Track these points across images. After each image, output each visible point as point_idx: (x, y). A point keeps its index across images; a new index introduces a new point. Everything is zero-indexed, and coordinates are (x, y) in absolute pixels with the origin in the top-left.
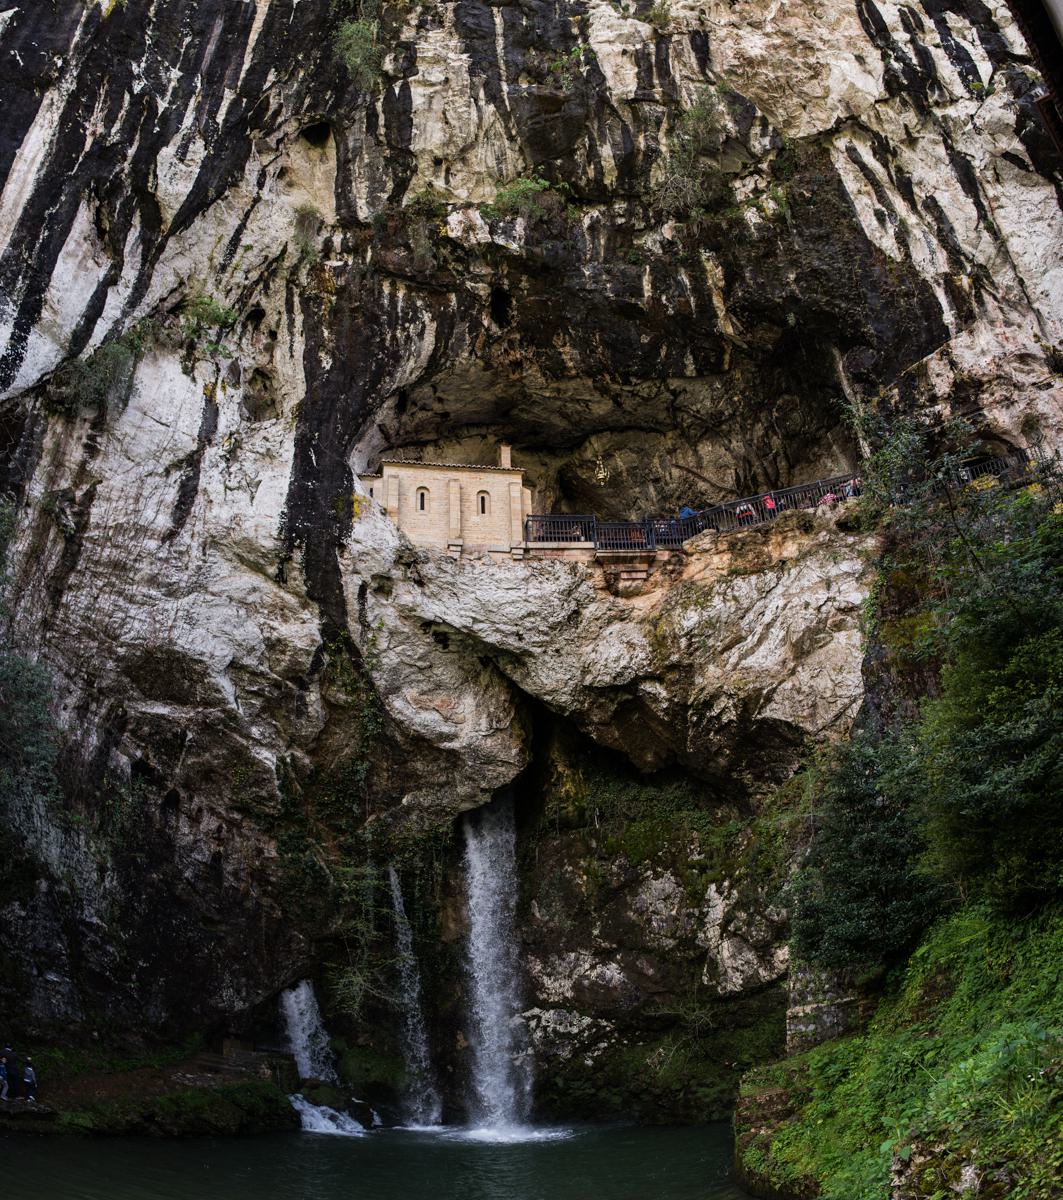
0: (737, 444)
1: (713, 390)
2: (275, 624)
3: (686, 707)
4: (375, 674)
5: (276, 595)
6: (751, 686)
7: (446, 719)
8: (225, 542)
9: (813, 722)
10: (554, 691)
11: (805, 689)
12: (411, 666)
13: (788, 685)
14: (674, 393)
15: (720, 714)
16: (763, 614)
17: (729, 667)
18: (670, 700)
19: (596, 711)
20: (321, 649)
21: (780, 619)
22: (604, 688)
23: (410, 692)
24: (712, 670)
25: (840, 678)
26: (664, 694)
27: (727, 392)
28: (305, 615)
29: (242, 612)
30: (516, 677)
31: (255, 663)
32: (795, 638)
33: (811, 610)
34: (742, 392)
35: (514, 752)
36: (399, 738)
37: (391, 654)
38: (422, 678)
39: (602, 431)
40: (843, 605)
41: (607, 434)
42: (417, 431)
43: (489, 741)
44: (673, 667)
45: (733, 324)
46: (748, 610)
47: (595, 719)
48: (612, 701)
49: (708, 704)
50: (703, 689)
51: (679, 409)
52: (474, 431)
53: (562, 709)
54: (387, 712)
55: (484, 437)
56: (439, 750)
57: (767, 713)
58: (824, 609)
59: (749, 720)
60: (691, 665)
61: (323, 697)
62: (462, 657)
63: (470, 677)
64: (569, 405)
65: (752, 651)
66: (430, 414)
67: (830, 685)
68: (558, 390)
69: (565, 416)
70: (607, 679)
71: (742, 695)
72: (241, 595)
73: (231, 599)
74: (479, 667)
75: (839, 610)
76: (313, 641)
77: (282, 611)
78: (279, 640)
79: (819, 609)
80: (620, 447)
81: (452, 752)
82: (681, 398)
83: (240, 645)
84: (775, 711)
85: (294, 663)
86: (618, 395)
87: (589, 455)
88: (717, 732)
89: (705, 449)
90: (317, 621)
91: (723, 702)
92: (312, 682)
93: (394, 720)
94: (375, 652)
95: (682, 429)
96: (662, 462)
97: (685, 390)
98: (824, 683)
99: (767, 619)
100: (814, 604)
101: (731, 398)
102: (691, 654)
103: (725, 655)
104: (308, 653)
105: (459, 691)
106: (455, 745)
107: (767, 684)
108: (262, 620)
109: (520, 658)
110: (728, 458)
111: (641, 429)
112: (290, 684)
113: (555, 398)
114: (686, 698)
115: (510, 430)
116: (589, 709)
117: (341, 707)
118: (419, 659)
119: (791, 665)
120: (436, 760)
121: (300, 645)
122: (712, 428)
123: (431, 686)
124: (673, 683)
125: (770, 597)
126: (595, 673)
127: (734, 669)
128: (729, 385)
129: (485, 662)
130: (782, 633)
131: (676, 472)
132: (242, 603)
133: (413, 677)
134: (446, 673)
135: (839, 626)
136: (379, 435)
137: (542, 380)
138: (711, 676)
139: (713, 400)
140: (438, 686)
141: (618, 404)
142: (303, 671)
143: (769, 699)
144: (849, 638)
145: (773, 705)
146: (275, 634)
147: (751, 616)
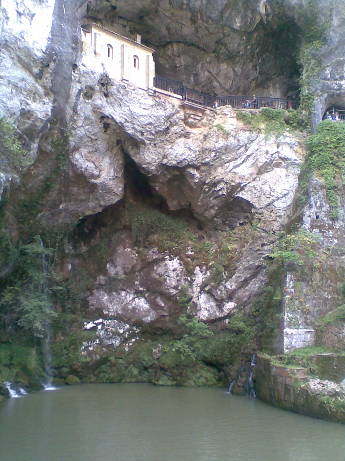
0: (238, 69)
1: (241, 40)
2: (29, 102)
3: (204, 183)
4: (71, 138)
5: (33, 85)
6: (237, 181)
7: (96, 167)
8: (12, 46)
9: (259, 204)
10: (150, 163)
11: (258, 188)
12: (89, 137)
13: (251, 185)
14: (224, 35)
15: (219, 190)
16: (247, 150)
17: (228, 170)
18: (199, 179)
19: (162, 177)
20: (49, 121)
21: (254, 155)
22: (171, 166)
23: (84, 151)
24: (220, 170)
25: (274, 187)
26: (198, 175)
27: (247, 42)
28: (46, 100)
29: (14, 91)
30: (132, 153)
31: (13, 122)
32: (260, 165)
33: (269, 155)
34: (252, 46)
35: (120, 189)
36: (71, 173)
37: (82, 130)
38: (91, 144)
39: (180, 42)
40: (283, 156)
41: (182, 44)
42: (99, 12)
43: (111, 183)
44: (205, 164)
45: (266, 9)
46: (242, 147)
47: (161, 181)
48: (170, 173)
49: (215, 184)
50: (215, 177)
51: (222, 44)
52: (121, 21)
53: (149, 172)
54: (70, 160)
55: (124, 27)
56: (88, 182)
57: (240, 195)
58: (274, 156)
59: (231, 196)
60: (212, 165)
61: (39, 148)
62: (110, 138)
63: (110, 149)
64: (174, 24)
65: (238, 166)
66: (109, 4)
67: (269, 190)
68: (173, 14)
69: (168, 29)
70: (175, 163)
71: (233, 184)
72: (16, 81)
73: (9, 82)
74: (115, 144)
75: (280, 158)
76: (47, 115)
77: (34, 95)
78: (29, 111)
79: (272, 155)
80: (185, 53)
81: (95, 184)
82: (226, 38)
83: (9, 110)
84: (244, 195)
85: (34, 125)
86: (200, 27)
87: (169, 53)
88: (215, 198)
89: (224, 66)
90: (51, 104)
91: (222, 185)
92: (38, 137)
93: (72, 164)
94: (75, 126)
95: (218, 54)
96: (203, 66)
97: (229, 35)
98: (266, 188)
99: (248, 153)
100: (271, 153)
101: (247, 46)
102: (214, 160)
103: (227, 164)
104: (42, 121)
105: (104, 155)
106: (97, 181)
107: (244, 182)
108: (23, 98)
109: (137, 144)
110: (232, 74)
111: (199, 48)
112: (25, 137)
113: (169, 18)
114: (206, 180)
115: (138, 27)
116: (160, 175)
117: (47, 153)
118: (94, 135)
119: (255, 176)
120: (84, 187)
121: (39, 116)
122: (231, 58)
123: (94, 150)
124: (203, 171)
125: (252, 144)
126: (169, 159)
127: (230, 172)
128: (248, 39)
129: (118, 142)
130: (254, 161)
131: (207, 73)
132: (15, 86)
133: (88, 143)
134: (101, 145)
135: (278, 165)
136: (86, 8)
137: (168, 6)
138: (219, 173)
139: (239, 44)
140: (97, 150)
141: (197, 30)
142: (35, 131)
143: (242, 189)
144: (281, 171)
145: (243, 192)
146: (28, 107)
147: (242, 150)
